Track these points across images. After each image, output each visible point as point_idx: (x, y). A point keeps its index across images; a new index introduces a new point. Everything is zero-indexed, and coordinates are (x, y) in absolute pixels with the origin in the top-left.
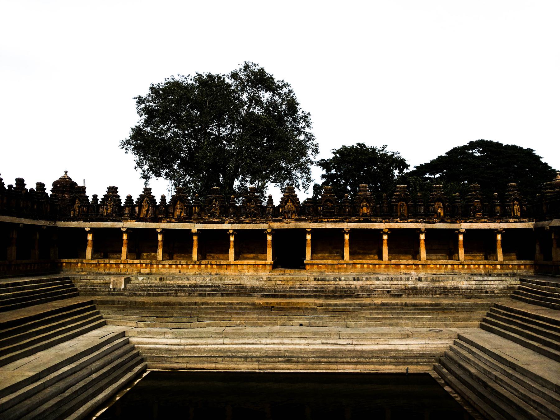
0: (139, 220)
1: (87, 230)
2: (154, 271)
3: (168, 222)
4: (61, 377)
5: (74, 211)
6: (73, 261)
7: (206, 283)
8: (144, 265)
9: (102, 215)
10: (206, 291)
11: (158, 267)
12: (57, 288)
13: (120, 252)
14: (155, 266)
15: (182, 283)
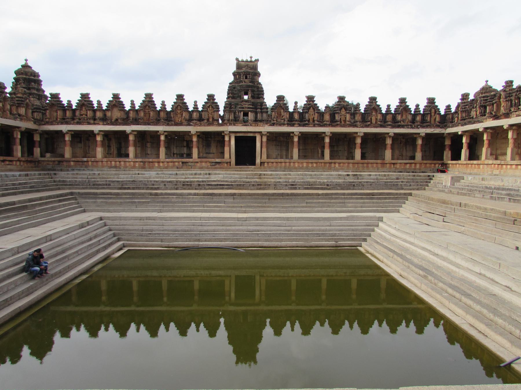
0: (496, 117)
1: (460, 133)
2: (502, 171)
3: (516, 116)
4: (261, 224)
5: (458, 118)
6: (454, 162)
7: (504, 186)
8: (496, 165)
9: (473, 118)
10: (501, 194)
11: (507, 168)
12: (402, 182)
13: (505, 154)
14: (504, 166)
15: (493, 185)
